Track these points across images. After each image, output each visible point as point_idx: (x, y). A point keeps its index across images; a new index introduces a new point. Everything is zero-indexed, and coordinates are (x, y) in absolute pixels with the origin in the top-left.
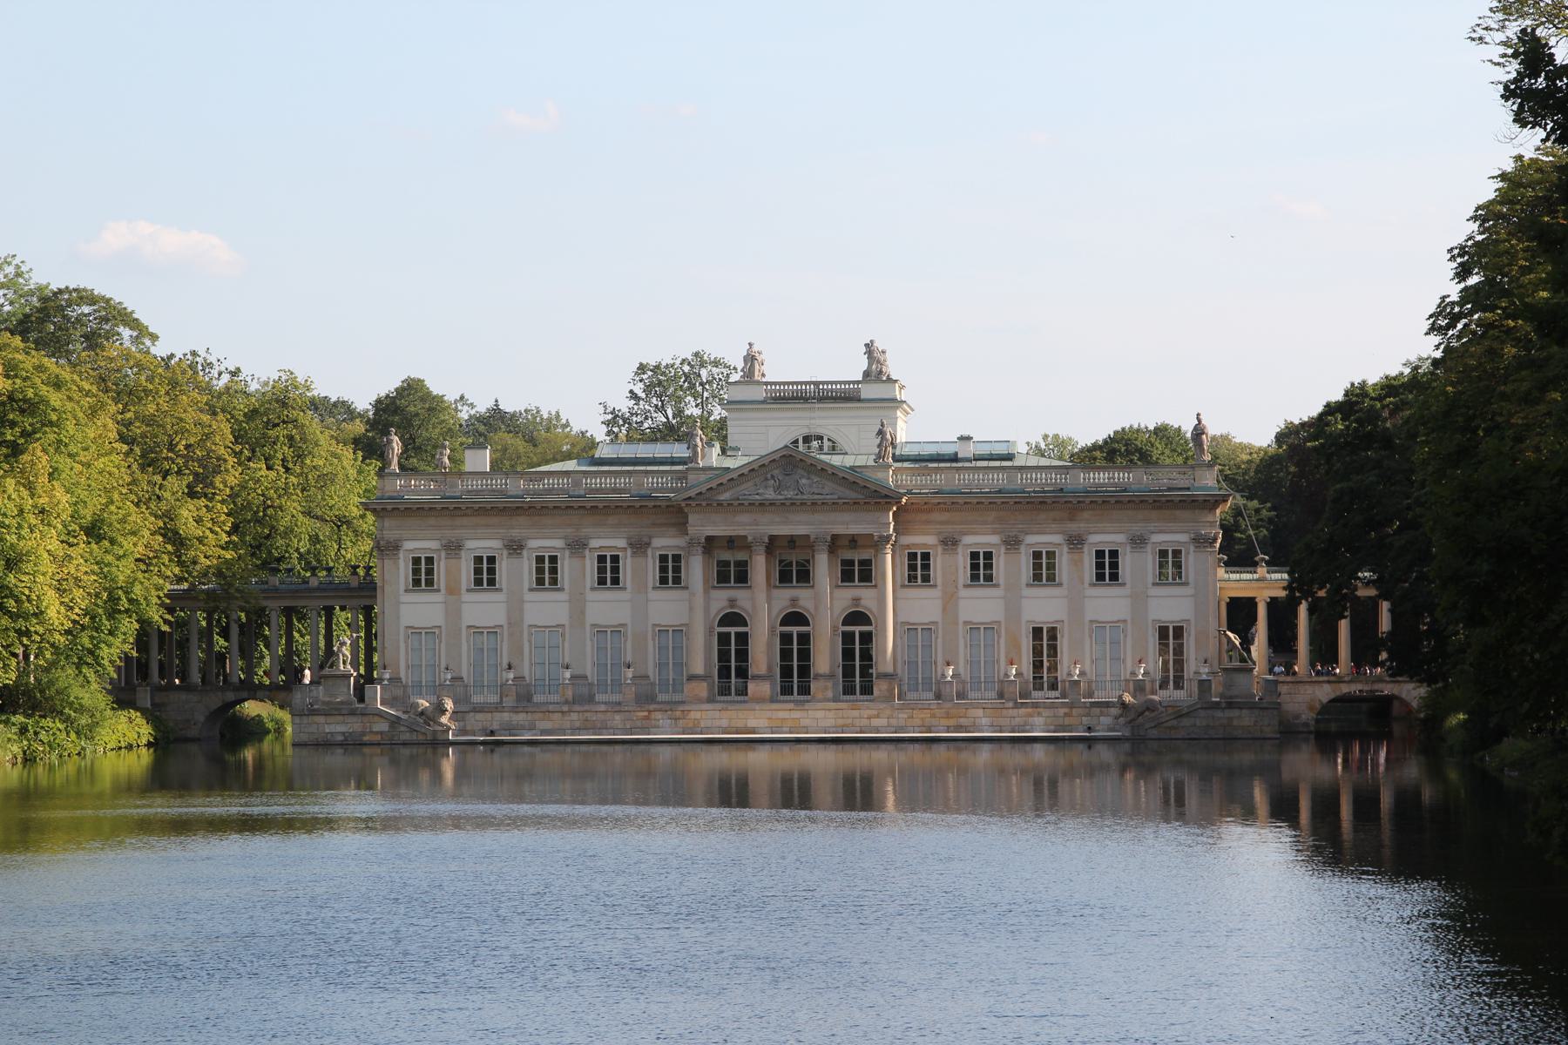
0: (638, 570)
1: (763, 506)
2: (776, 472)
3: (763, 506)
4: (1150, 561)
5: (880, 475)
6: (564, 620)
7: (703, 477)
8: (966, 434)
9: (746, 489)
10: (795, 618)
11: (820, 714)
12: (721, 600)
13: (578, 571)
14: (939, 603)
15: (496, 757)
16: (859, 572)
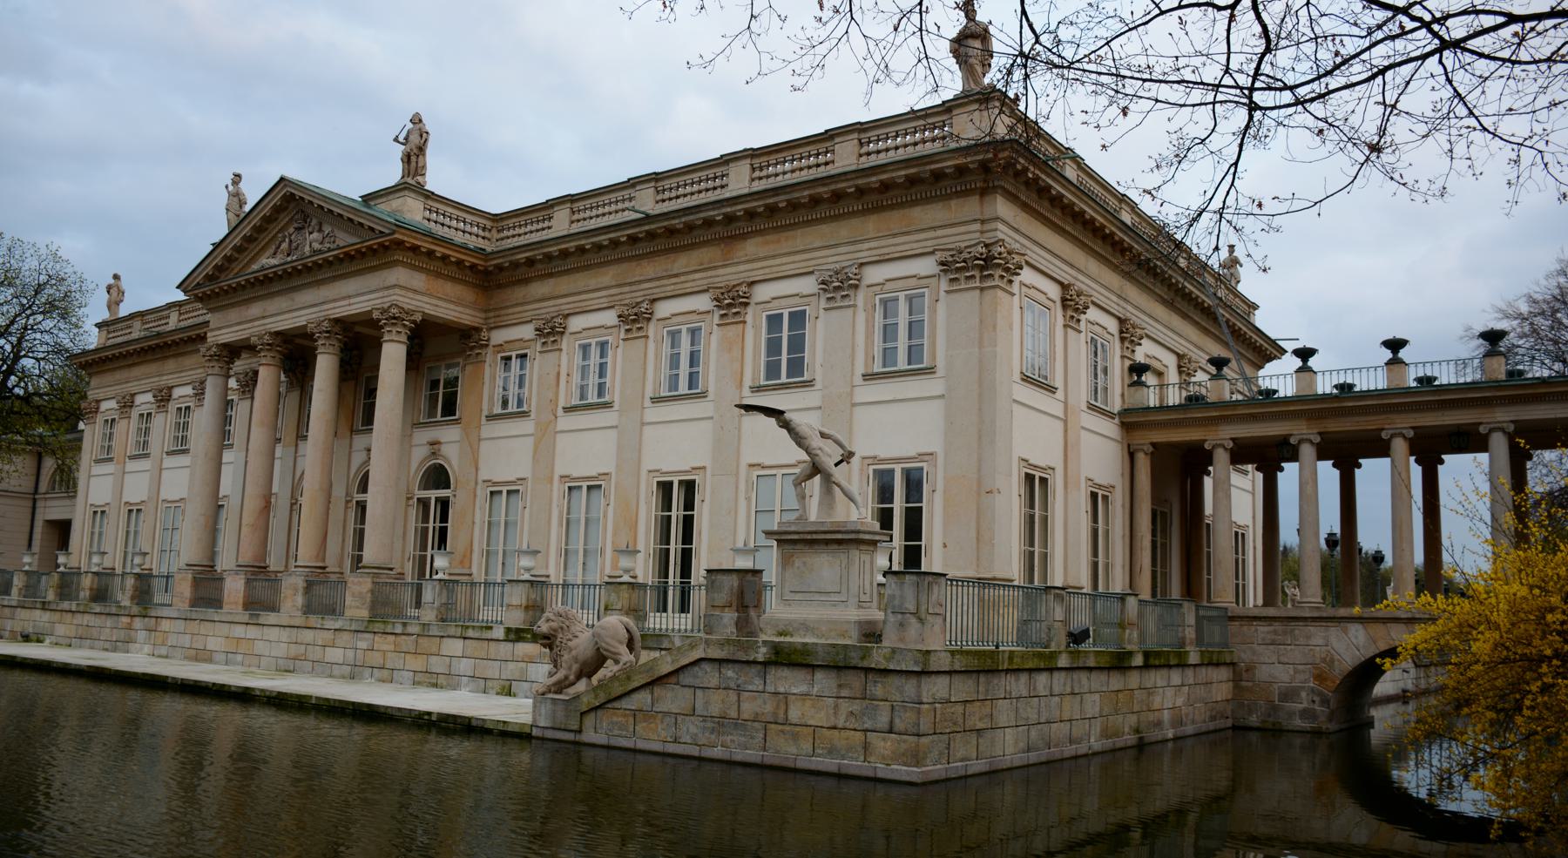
11: (273, 633)
14: (530, 441)
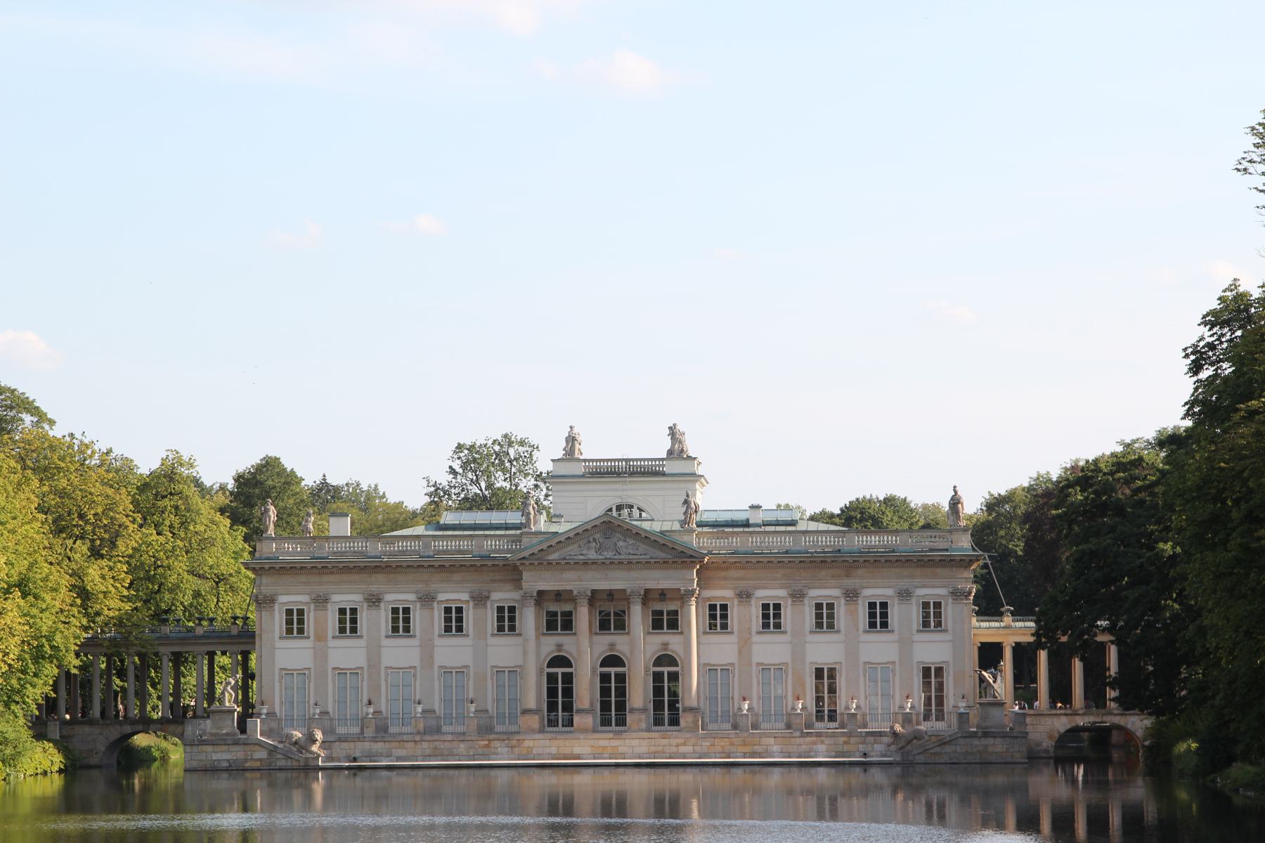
0: (479, 620)
1: (586, 564)
2: (597, 536)
3: (586, 564)
4: (915, 613)
5: (685, 538)
6: (416, 663)
7: (535, 540)
8: (756, 503)
9: (572, 551)
10: (612, 660)
11: (635, 743)
12: (549, 645)
13: (427, 621)
14: (735, 647)
15: (358, 781)
16: (666, 621)
